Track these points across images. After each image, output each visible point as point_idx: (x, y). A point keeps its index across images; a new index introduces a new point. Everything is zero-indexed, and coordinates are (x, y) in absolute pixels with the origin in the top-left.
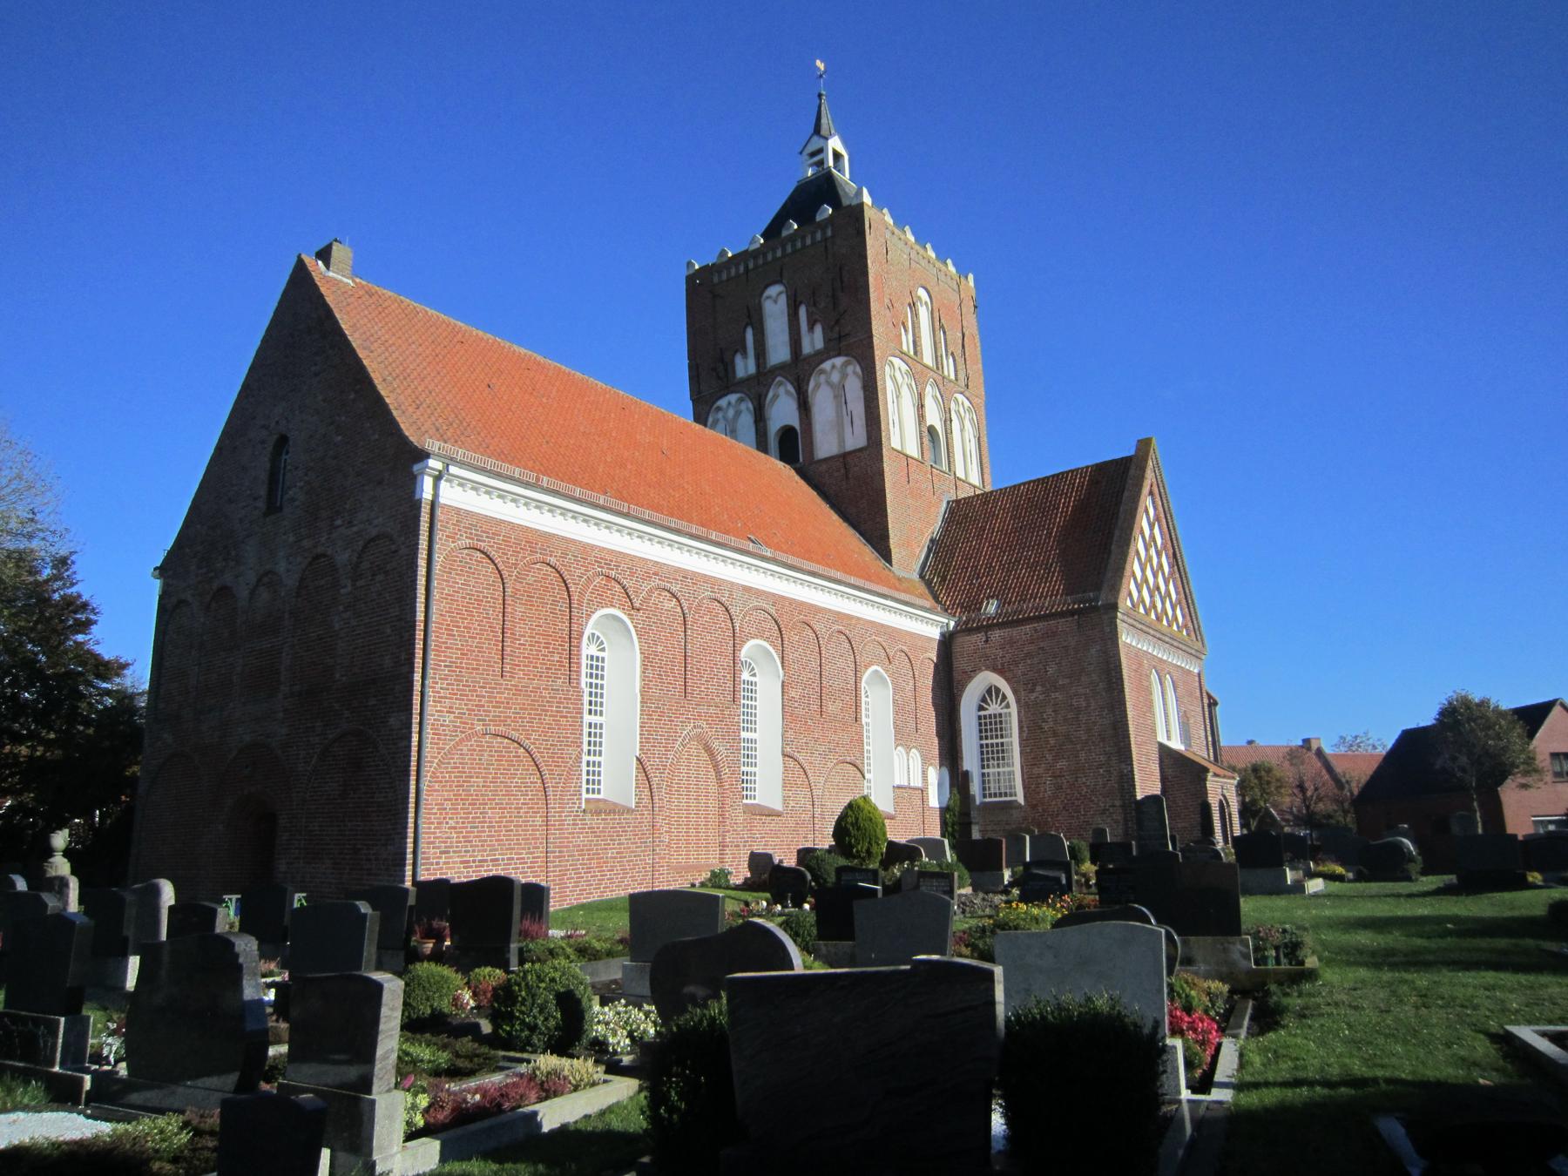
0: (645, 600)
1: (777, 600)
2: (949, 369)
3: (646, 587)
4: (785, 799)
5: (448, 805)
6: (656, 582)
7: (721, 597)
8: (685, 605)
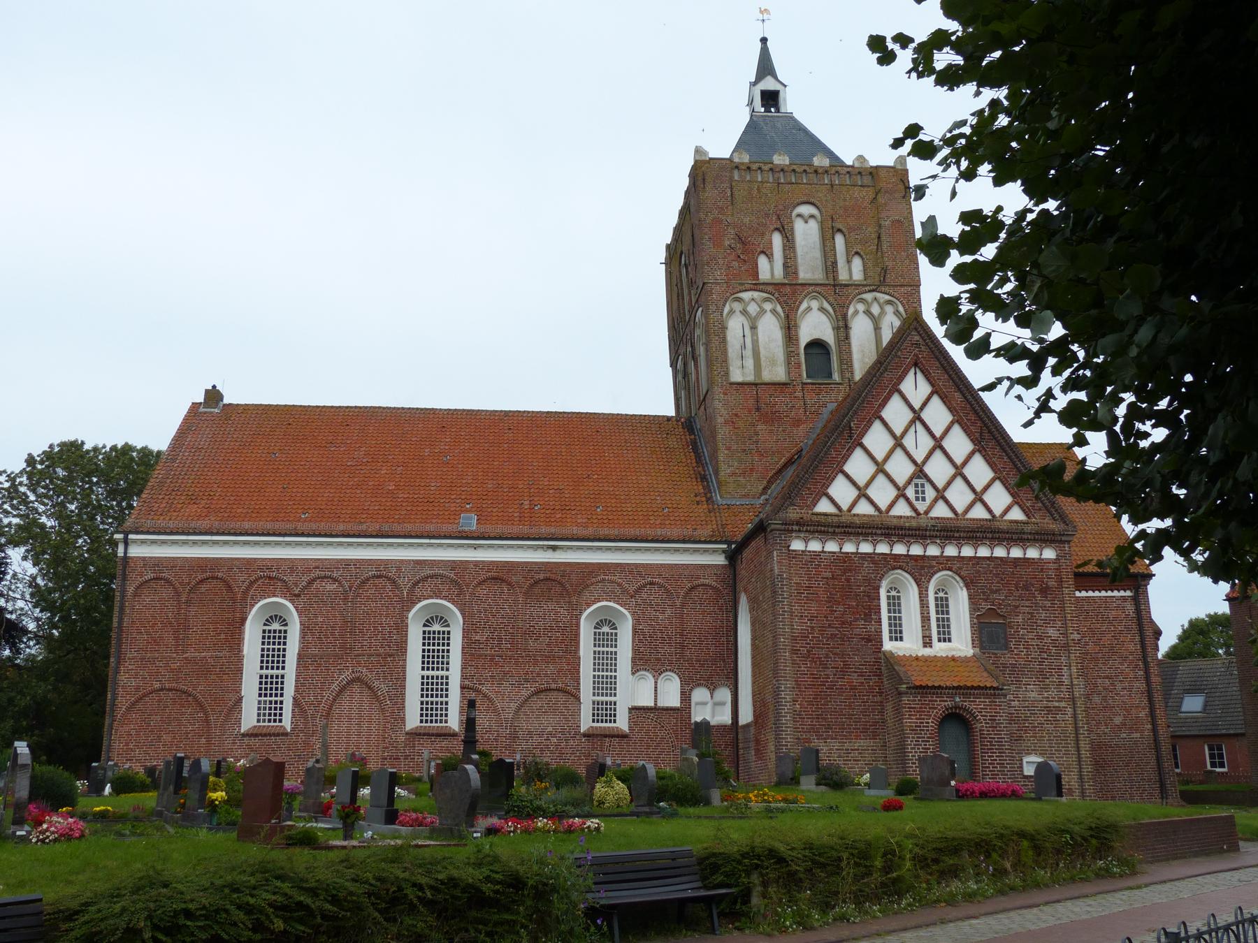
0: (305, 587)
1: (453, 565)
2: (856, 271)
3: (306, 579)
5: (133, 732)
7: (382, 573)
8: (346, 585)
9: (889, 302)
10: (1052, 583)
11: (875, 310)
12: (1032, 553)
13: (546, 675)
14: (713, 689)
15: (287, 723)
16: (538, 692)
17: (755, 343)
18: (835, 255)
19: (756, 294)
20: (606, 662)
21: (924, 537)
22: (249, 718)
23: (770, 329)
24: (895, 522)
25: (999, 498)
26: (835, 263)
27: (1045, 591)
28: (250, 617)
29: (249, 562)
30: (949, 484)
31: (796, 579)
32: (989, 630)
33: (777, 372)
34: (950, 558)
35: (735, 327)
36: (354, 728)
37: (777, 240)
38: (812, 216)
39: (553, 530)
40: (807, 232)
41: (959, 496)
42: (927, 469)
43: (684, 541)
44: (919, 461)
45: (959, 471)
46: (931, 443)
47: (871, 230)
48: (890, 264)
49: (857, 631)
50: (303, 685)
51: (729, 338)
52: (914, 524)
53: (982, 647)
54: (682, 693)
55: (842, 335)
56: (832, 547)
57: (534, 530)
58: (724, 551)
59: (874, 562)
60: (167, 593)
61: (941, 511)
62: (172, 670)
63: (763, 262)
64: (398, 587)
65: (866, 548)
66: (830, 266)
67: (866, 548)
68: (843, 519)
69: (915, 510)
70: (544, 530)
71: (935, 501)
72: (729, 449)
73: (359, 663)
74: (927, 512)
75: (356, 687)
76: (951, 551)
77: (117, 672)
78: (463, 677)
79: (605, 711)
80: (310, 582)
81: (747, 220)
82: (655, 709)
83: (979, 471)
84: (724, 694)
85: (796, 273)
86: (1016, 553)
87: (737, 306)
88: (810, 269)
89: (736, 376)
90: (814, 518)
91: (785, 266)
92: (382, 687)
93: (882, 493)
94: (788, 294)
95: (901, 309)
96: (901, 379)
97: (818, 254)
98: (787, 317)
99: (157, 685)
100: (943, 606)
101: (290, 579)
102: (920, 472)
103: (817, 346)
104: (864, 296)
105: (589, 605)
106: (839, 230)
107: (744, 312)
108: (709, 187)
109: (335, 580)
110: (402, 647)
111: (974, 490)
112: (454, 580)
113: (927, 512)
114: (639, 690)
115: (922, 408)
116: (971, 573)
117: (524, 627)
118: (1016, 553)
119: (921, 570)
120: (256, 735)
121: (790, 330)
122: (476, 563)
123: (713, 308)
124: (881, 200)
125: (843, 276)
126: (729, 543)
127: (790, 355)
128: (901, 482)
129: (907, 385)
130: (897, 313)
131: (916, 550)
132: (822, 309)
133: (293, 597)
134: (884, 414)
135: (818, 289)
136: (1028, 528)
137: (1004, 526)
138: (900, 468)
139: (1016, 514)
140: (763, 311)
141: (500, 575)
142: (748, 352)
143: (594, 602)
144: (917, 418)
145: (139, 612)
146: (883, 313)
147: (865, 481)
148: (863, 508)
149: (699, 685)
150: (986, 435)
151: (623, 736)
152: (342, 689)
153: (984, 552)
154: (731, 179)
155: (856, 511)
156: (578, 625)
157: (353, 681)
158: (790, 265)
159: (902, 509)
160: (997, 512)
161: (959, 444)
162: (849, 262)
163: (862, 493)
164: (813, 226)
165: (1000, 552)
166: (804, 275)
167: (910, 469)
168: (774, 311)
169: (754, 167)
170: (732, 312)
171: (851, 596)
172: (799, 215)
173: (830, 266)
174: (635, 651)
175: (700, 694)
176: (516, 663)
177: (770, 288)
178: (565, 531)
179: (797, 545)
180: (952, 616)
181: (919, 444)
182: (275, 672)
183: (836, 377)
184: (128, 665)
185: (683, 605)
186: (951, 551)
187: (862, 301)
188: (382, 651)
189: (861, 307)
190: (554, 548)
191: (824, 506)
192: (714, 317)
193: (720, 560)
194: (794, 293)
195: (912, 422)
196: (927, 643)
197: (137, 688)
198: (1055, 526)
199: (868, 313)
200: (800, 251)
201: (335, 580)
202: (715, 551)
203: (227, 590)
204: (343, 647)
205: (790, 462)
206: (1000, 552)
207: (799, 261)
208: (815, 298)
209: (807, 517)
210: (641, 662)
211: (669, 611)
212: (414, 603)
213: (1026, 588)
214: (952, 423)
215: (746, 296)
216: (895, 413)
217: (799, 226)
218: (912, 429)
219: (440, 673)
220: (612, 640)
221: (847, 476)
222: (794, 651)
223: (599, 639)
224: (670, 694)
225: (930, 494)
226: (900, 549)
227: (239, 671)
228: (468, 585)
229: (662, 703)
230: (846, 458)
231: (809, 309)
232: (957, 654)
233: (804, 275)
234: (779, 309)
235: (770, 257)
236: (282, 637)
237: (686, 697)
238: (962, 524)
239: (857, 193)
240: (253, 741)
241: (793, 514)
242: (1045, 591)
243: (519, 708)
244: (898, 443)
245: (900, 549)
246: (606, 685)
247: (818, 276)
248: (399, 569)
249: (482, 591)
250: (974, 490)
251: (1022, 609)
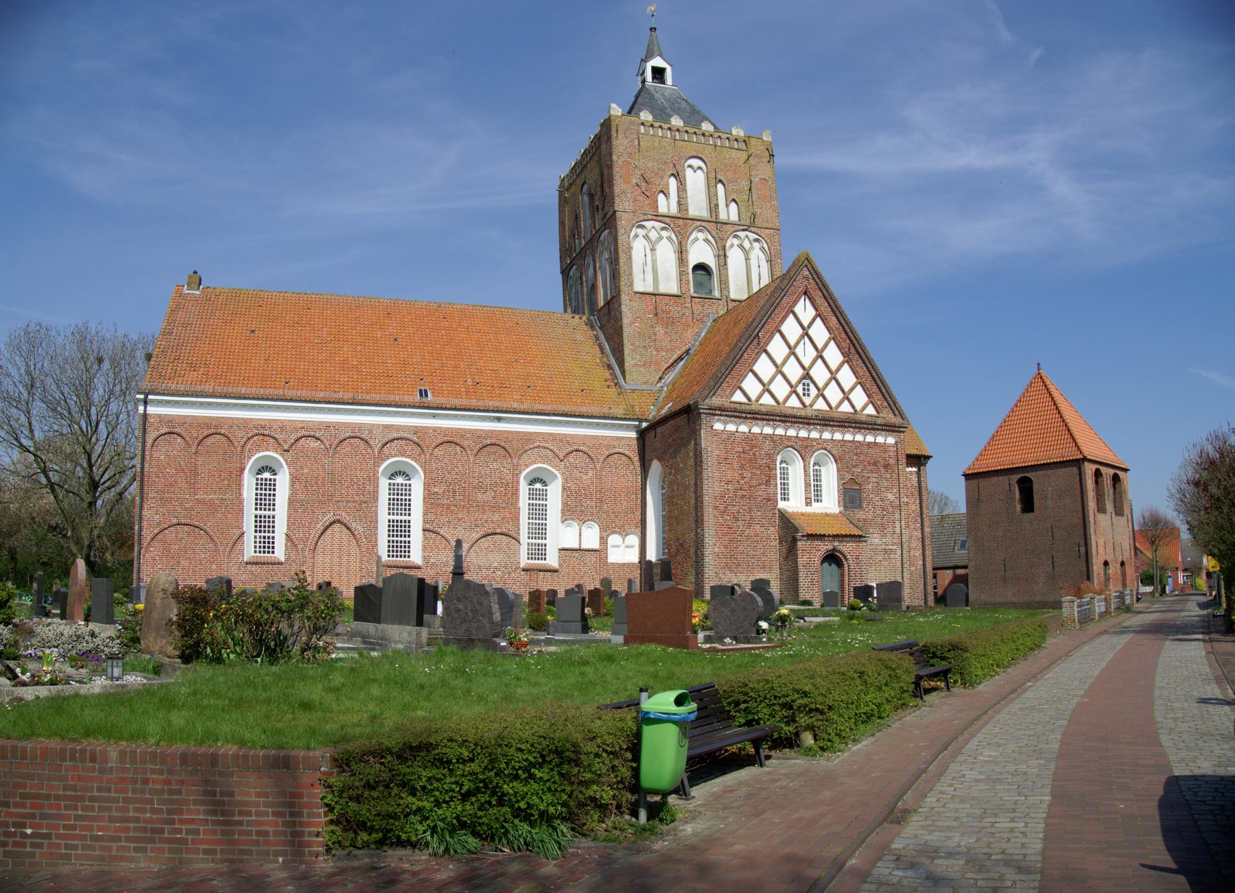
1: (416, 430)
2: (730, 213)
3: (294, 437)
4: (424, 558)
6: (303, 432)
9: (756, 240)
10: (892, 461)
11: (746, 244)
12: (880, 439)
13: (492, 522)
14: (624, 534)
15: (280, 553)
17: (654, 262)
20: (539, 512)
21: (809, 424)
22: (249, 550)
23: (666, 252)
24: (790, 412)
25: (859, 397)
26: (717, 206)
27: (886, 466)
28: (248, 467)
30: (827, 385)
31: (717, 452)
32: (851, 496)
33: (672, 287)
34: (825, 441)
35: (639, 248)
36: (336, 560)
37: (673, 182)
38: (700, 168)
39: (497, 404)
40: (696, 180)
41: (833, 394)
42: (812, 373)
43: (605, 418)
44: (807, 365)
45: (833, 377)
47: (745, 184)
48: (758, 211)
49: (760, 493)
50: (294, 524)
51: (634, 257)
52: (803, 413)
53: (845, 507)
54: (601, 538)
55: (722, 261)
56: (743, 428)
57: (480, 404)
58: (635, 426)
59: (773, 441)
61: (821, 405)
62: (186, 509)
65: (768, 430)
66: (713, 208)
67: (768, 430)
68: (753, 407)
69: (803, 403)
70: (491, 404)
71: (817, 397)
72: (633, 344)
73: (339, 508)
74: (811, 405)
75: (337, 526)
76: (827, 435)
77: (141, 508)
78: (425, 521)
79: (540, 551)
81: (650, 165)
83: (847, 377)
84: (634, 540)
86: (870, 439)
87: (641, 232)
88: (697, 206)
89: (639, 287)
90: (732, 406)
91: (679, 204)
92: (358, 527)
93: (780, 389)
94: (681, 224)
95: (765, 246)
96: (795, 303)
98: (680, 243)
99: (175, 521)
100: (817, 477)
102: (807, 376)
103: (701, 268)
105: (527, 466)
106: (720, 181)
107: (646, 237)
108: (621, 136)
109: (317, 439)
111: (843, 391)
113: (811, 405)
114: (564, 535)
116: (842, 455)
117: (474, 485)
118: (870, 439)
119: (805, 448)
120: (257, 563)
121: (682, 253)
122: (435, 429)
123: (621, 231)
124: (752, 161)
126: (641, 421)
127: (682, 274)
128: (793, 382)
130: (762, 249)
131: (803, 434)
132: (706, 240)
134: (783, 328)
135: (704, 224)
136: (879, 421)
137: (864, 419)
138: (793, 371)
139: (870, 410)
140: (661, 238)
142: (649, 269)
143: (531, 464)
144: (806, 334)
146: (752, 248)
147: (768, 378)
148: (767, 400)
149: (614, 532)
150: (853, 350)
151: (556, 571)
153: (848, 437)
154: (638, 131)
155: (761, 401)
156: (518, 482)
157: (334, 522)
158: (682, 203)
159: (794, 402)
160: (858, 408)
161: (834, 355)
163: (766, 389)
164: (700, 175)
165: (859, 438)
167: (800, 372)
168: (669, 238)
169: (656, 124)
170: (636, 236)
171: (759, 466)
172: (690, 166)
173: (713, 208)
174: (565, 504)
175: (614, 539)
176: (468, 512)
177: (667, 220)
178: (505, 405)
179: (718, 426)
180: (823, 483)
181: (807, 353)
182: (267, 513)
183: (717, 294)
185: (602, 468)
186: (827, 435)
188: (357, 498)
190: (499, 419)
192: (621, 239)
193: (633, 435)
194: (686, 225)
196: (808, 503)
197: (159, 524)
198: (897, 420)
199: (741, 246)
201: (317, 439)
202: (627, 428)
203: (227, 445)
205: (680, 359)
206: (859, 438)
208: (700, 231)
209: (727, 405)
211: (591, 473)
213: (875, 464)
214: (830, 339)
215: (648, 224)
216: (790, 328)
217: (689, 172)
219: (403, 518)
220: (543, 495)
221: (756, 375)
222: (716, 508)
223: (533, 494)
224: (591, 537)
225: (813, 392)
226: (792, 432)
227: (242, 511)
228: (428, 447)
229: (584, 546)
230: (755, 360)
231: (697, 239)
232: (829, 511)
233: (692, 212)
234: (673, 237)
235: (666, 195)
236: (272, 485)
237: (603, 541)
238: (834, 415)
239: (734, 154)
240: (254, 568)
241: (716, 401)
242: (886, 466)
244: (792, 352)
245: (792, 432)
246: (540, 531)
247: (704, 213)
248: (371, 431)
250: (843, 391)
251: (872, 480)
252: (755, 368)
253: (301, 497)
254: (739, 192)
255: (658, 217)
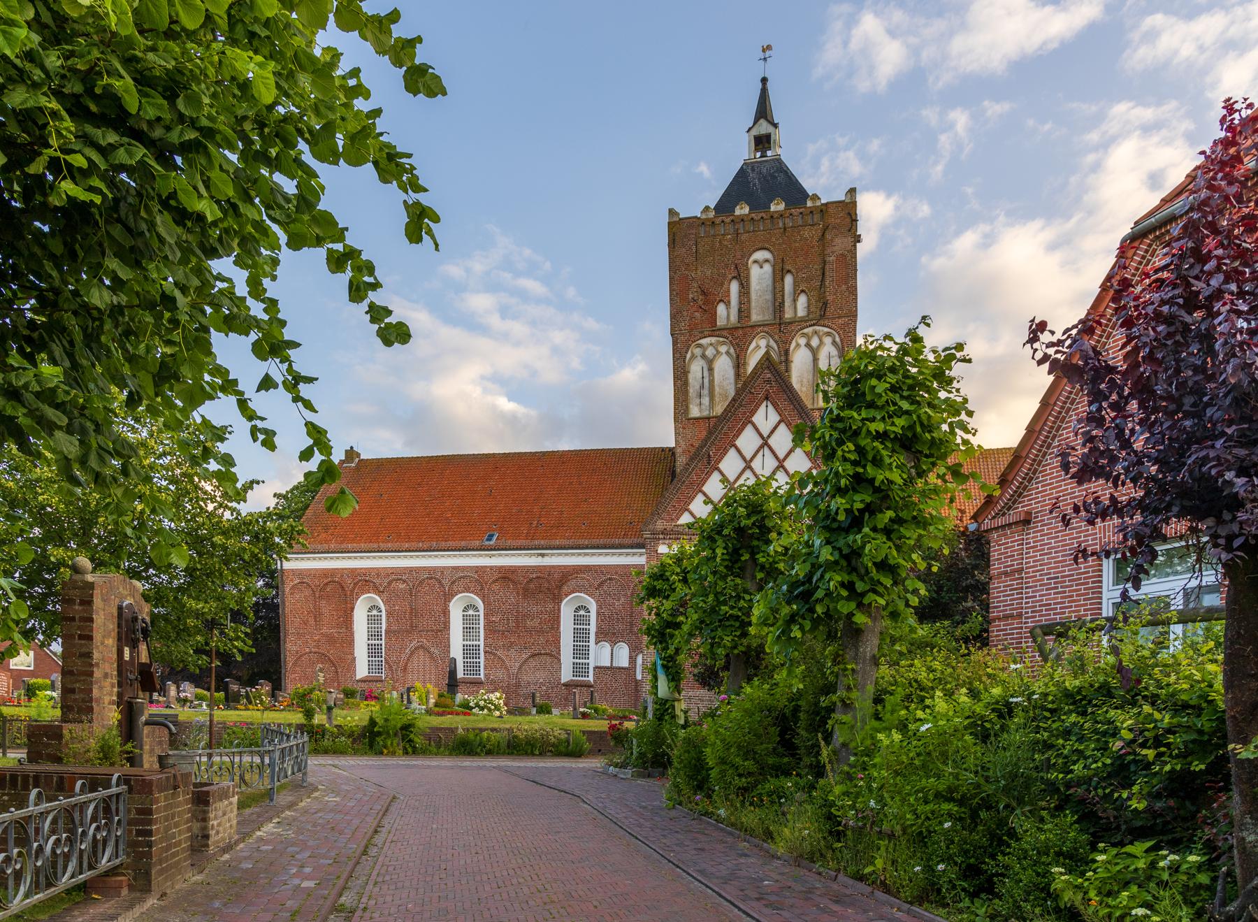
1: (478, 569)
7: (433, 574)
9: (828, 334)
16: (533, 656)
18: (783, 296)
19: (713, 340)
26: (782, 304)
29: (353, 570)
46: (776, 464)
60: (307, 592)
63: (721, 309)
64: (443, 586)
66: (778, 306)
80: (390, 583)
82: (611, 668)
85: (749, 317)
91: (740, 311)
96: (753, 412)
97: (769, 297)
101: (377, 581)
104: (805, 331)
110: (446, 626)
112: (478, 580)
115: (769, 436)
122: (491, 568)
125: (788, 315)
129: (759, 418)
133: (380, 593)
141: (507, 575)
144: (765, 443)
145: (293, 606)
152: (412, 653)
158: (744, 312)
162: (795, 301)
166: (755, 317)
168: (727, 353)
173: (778, 307)
184: (290, 638)
187: (804, 335)
189: (803, 341)
191: (685, 519)
194: (745, 335)
195: (762, 447)
199: (808, 345)
200: (753, 296)
203: (342, 590)
204: (411, 626)
207: (753, 304)
210: (602, 635)
212: (453, 596)
216: (747, 441)
218: (761, 453)
224: (622, 656)
230: (704, 481)
235: (728, 304)
241: (660, 525)
243: (520, 667)
247: (768, 317)
249: (496, 587)
252: (705, 489)
253: (394, 628)
254: (808, 280)
255: (715, 331)
